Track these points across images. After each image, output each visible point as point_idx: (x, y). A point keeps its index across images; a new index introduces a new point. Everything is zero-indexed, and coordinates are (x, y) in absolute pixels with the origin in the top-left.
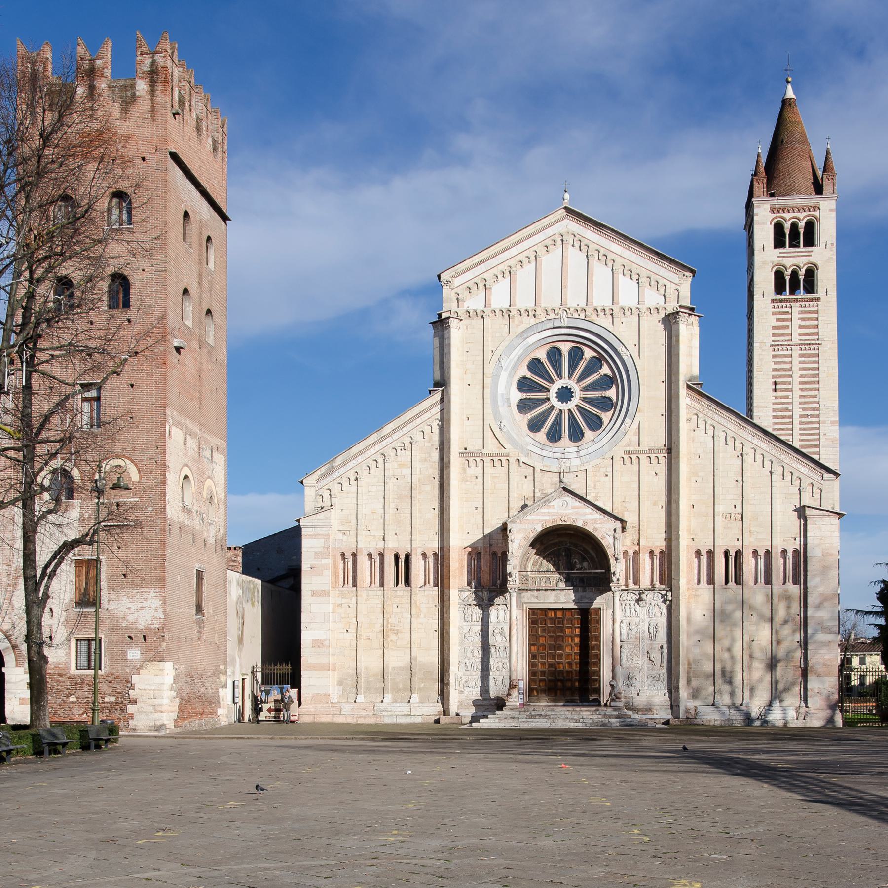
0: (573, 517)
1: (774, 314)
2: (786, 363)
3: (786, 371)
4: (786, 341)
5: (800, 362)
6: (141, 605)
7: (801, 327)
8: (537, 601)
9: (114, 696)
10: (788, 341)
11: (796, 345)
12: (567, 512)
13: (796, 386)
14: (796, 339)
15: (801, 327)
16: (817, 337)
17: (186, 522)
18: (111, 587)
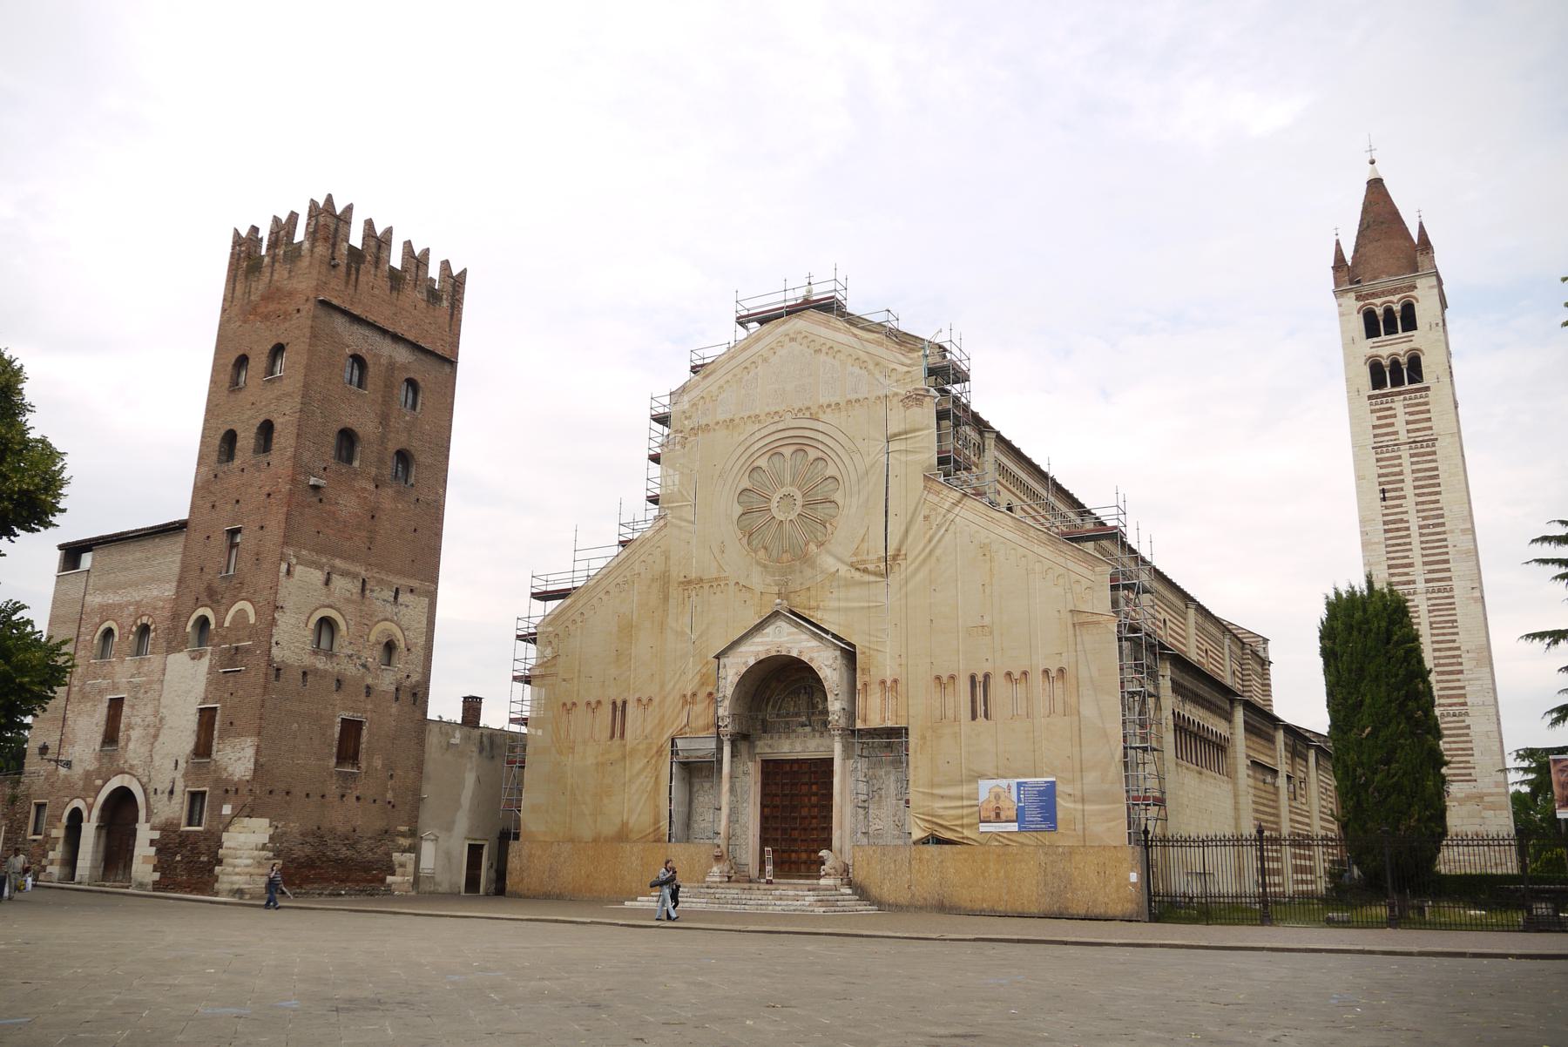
0: (789, 645)
1: (1373, 411)
2: (1395, 466)
3: (1395, 475)
4: (1391, 440)
5: (1412, 463)
6: (239, 755)
7: (1408, 423)
8: (769, 751)
9: (208, 856)
10: (1395, 440)
11: (1406, 444)
12: (782, 639)
13: (1409, 489)
14: (1403, 437)
15: (1408, 423)
16: (1430, 432)
17: (320, 666)
18: (220, 737)
